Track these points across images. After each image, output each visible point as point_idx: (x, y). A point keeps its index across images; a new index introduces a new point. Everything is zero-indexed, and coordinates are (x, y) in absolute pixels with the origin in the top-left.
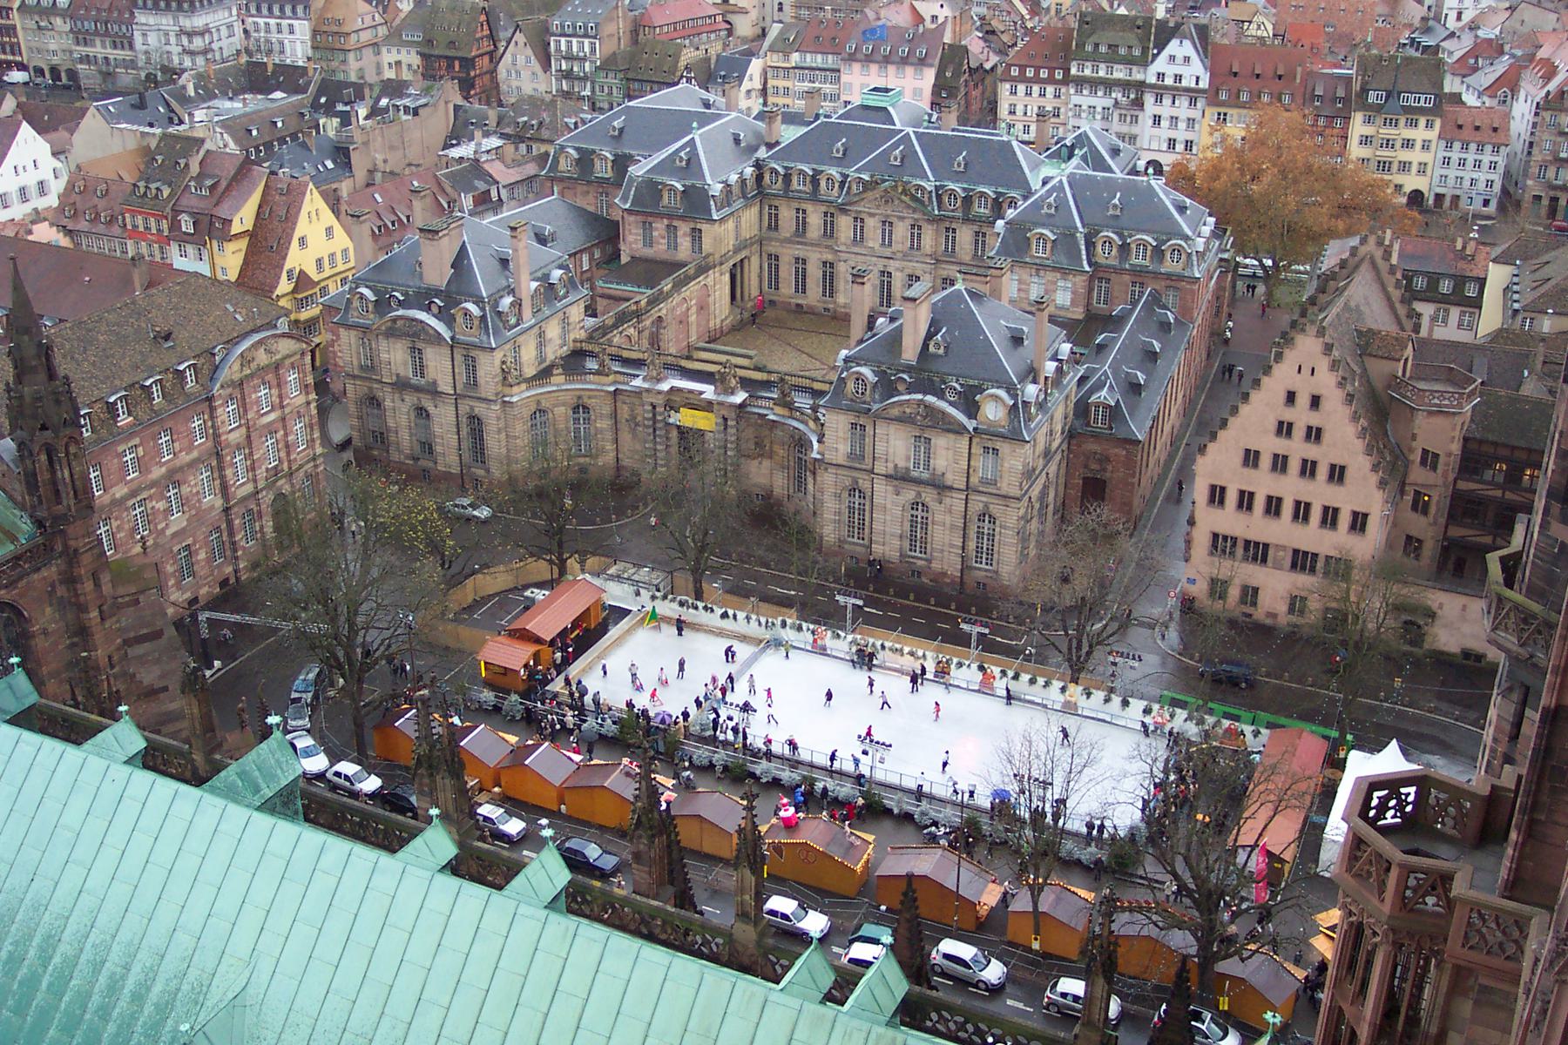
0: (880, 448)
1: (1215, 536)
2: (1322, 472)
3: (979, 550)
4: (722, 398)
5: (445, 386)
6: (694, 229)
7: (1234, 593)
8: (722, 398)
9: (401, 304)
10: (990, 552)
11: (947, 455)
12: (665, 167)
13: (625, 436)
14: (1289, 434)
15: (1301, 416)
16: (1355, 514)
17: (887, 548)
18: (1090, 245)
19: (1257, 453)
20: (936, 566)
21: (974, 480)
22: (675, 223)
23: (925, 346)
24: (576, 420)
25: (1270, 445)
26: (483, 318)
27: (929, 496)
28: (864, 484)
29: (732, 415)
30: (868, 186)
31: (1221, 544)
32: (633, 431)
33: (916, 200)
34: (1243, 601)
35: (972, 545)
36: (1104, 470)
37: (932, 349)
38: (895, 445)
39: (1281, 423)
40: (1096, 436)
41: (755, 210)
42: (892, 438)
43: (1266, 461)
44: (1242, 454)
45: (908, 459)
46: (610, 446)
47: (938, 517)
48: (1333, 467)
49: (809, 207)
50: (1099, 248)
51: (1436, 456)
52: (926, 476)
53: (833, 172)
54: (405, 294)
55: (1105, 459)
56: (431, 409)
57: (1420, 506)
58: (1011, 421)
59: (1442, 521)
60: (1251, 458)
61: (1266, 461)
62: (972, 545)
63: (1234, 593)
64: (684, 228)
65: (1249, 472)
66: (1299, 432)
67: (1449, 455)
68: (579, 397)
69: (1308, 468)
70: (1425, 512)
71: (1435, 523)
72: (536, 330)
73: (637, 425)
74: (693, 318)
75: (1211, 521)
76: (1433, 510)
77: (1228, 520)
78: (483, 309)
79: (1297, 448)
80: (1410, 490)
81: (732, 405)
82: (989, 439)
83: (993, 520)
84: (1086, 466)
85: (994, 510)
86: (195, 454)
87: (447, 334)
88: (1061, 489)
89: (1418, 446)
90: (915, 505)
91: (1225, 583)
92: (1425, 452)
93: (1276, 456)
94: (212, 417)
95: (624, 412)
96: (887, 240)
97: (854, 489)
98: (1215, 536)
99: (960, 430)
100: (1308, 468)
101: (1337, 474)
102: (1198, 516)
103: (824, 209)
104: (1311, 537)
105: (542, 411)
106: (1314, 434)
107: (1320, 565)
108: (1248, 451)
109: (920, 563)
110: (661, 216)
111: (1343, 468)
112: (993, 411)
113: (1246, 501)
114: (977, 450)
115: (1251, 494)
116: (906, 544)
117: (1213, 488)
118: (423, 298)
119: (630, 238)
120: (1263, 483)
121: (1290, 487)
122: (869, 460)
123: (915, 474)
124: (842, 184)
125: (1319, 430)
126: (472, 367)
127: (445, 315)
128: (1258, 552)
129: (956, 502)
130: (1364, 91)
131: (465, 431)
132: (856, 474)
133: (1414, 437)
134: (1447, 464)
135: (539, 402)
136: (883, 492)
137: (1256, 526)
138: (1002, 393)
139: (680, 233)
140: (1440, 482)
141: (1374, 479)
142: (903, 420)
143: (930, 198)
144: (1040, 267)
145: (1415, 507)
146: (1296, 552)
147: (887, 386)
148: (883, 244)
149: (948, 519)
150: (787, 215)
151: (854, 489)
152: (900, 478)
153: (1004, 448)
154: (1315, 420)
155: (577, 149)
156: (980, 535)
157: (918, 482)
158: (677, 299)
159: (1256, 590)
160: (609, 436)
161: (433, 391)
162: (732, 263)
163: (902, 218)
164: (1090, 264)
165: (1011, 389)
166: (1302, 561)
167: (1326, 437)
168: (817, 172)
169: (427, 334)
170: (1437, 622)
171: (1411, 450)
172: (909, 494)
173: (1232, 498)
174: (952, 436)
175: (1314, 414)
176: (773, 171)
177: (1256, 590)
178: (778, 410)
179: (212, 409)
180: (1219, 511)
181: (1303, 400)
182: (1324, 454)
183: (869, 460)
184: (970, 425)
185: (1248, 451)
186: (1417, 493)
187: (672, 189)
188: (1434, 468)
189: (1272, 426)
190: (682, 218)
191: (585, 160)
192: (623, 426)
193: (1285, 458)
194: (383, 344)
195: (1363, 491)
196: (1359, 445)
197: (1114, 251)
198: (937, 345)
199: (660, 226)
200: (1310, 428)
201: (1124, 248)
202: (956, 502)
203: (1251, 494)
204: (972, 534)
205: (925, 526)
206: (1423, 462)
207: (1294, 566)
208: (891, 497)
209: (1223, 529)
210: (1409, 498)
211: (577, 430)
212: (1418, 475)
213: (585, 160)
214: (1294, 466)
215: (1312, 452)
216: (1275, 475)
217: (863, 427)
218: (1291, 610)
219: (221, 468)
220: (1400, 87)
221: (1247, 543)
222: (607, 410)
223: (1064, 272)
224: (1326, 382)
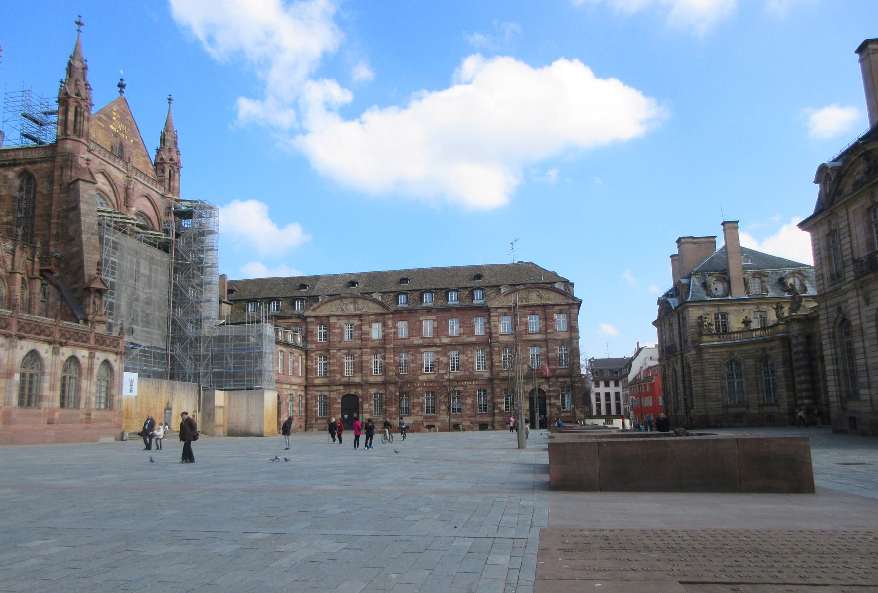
17: (873, 391)
42: (852, 225)
68: (764, 349)
86: (473, 339)
94: (489, 322)
105: (738, 364)
135: (731, 353)
179: (490, 317)
219: (491, 355)
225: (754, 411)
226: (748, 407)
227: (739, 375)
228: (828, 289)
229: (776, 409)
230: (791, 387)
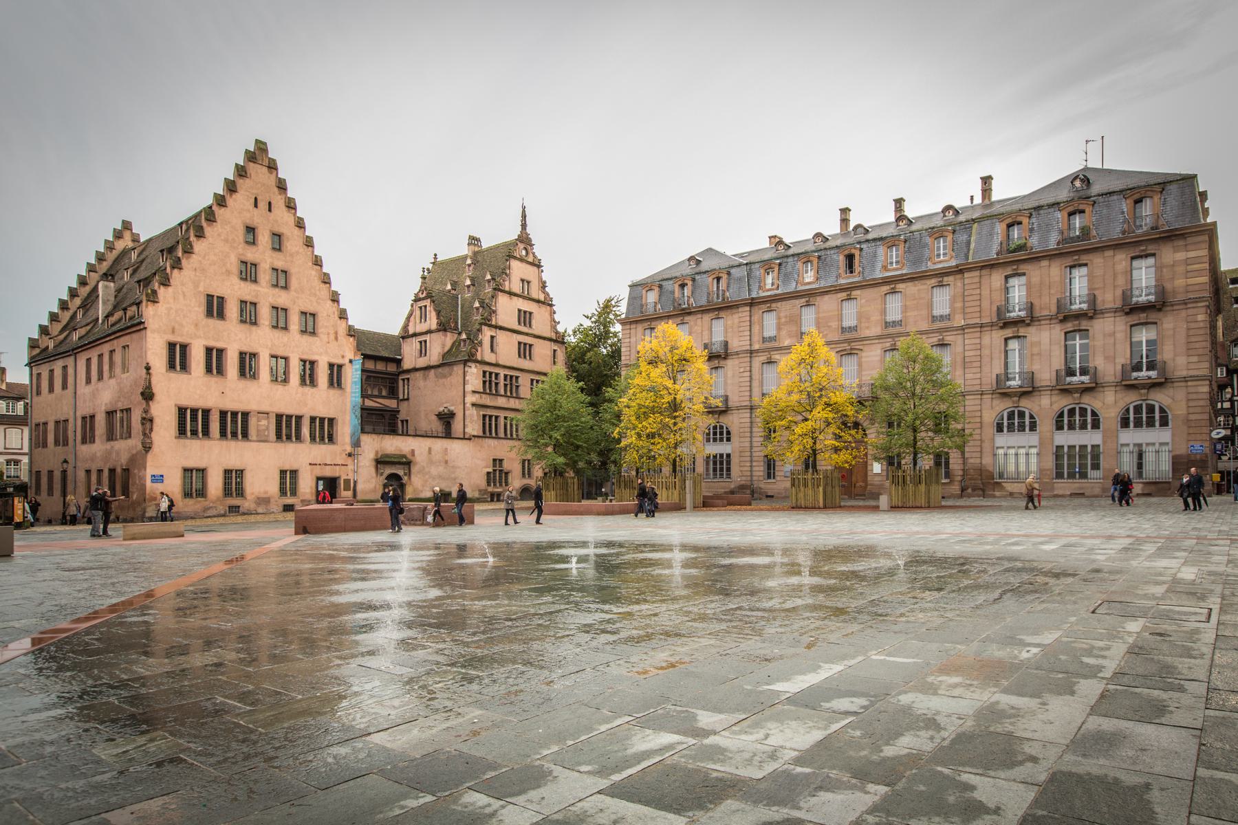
2: (295, 322)
7: (215, 484)
19: (221, 300)
25: (234, 290)
34: (227, 492)
44: (203, 300)
60: (215, 307)
61: (232, 310)
63: (215, 484)
66: (265, 276)
75: (176, 391)
77: (194, 387)
79: (265, 295)
98: (182, 411)
100: (280, 319)
102: (157, 388)
106: (282, 279)
107: (305, 431)
108: (210, 297)
113: (215, 360)
115: (221, 352)
120: (233, 337)
128: (235, 425)
137: (230, 393)
146: (279, 417)
159: (240, 473)
166: (287, 427)
170: (414, 469)
173: (197, 358)
177: (240, 473)
180: (183, 377)
181: (264, 238)
185: (210, 297)
203: (221, 352)
207: (279, 436)
209: (190, 401)
215: (282, 298)
218: (283, 492)
221: (223, 414)
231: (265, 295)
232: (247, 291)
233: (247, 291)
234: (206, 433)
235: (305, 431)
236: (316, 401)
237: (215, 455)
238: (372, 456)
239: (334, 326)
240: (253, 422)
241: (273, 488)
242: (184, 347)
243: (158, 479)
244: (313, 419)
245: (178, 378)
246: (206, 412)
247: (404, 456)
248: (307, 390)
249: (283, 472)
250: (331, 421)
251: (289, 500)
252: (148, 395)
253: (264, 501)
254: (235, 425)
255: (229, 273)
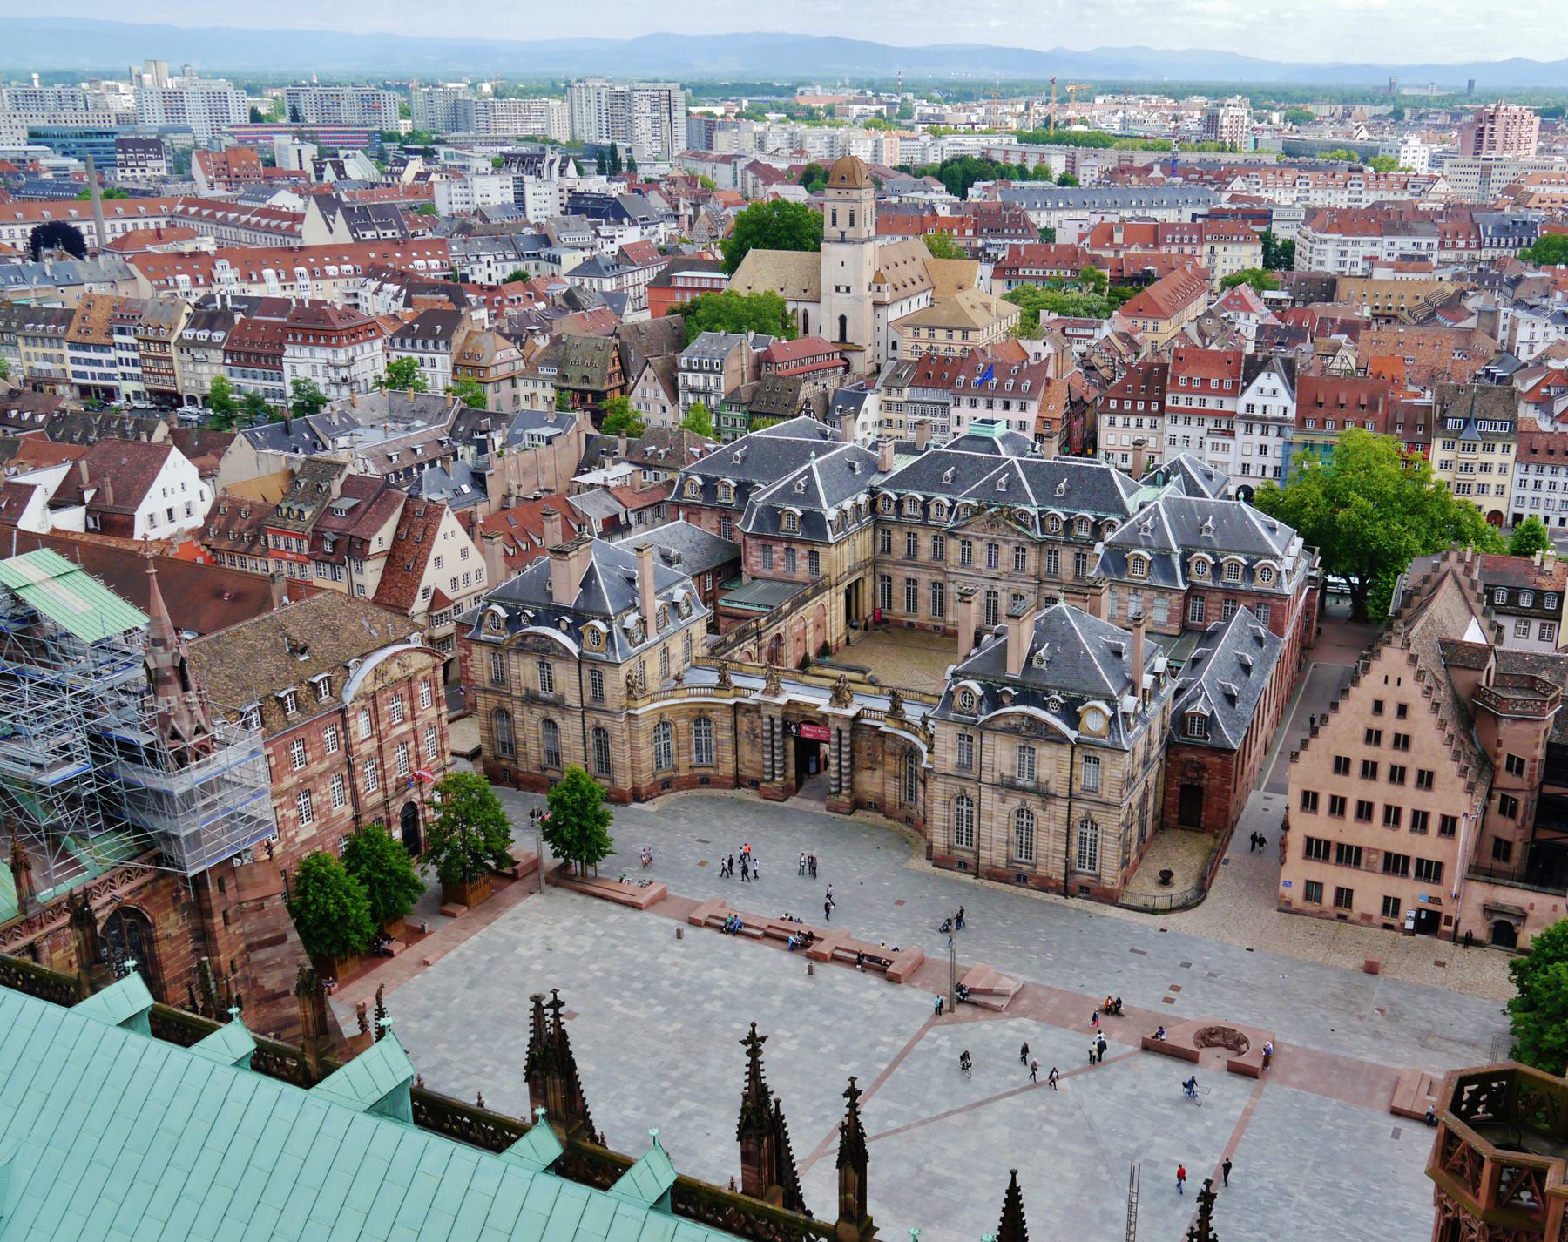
0: (987, 758)
1: (1309, 840)
2: (1411, 777)
3: (1082, 855)
4: (837, 711)
5: (572, 700)
6: (811, 553)
8: (837, 711)
9: (532, 621)
10: (1093, 857)
11: (1050, 764)
12: (787, 493)
13: (746, 751)
14: (1378, 741)
15: (1389, 724)
16: (1444, 818)
17: (994, 854)
18: (1185, 565)
19: (1347, 760)
20: (1041, 871)
21: (1076, 788)
22: (794, 546)
23: (1029, 661)
24: (698, 732)
25: (1359, 752)
26: (610, 635)
27: (1033, 803)
28: (972, 792)
29: (846, 727)
30: (977, 512)
31: (1316, 849)
32: (752, 743)
33: (1019, 519)
35: (1075, 850)
36: (1201, 778)
37: (1035, 664)
38: (1000, 755)
39: (1369, 732)
40: (1194, 747)
41: (869, 534)
42: (998, 747)
43: (1356, 768)
44: (1332, 760)
45: (1013, 768)
46: (729, 758)
47: (1043, 824)
48: (1421, 773)
49: (920, 532)
50: (1193, 568)
51: (1521, 761)
52: (1030, 784)
53: (944, 499)
54: (536, 612)
55: (1202, 767)
56: (559, 721)
57: (1508, 808)
58: (1111, 731)
59: (1530, 824)
60: (1342, 765)
61: (1356, 768)
62: (1075, 850)
63: (1329, 896)
64: (802, 551)
65: (1340, 779)
66: (1387, 740)
67: (1534, 760)
68: (701, 710)
69: (1397, 775)
70: (1513, 815)
71: (1523, 825)
72: (660, 647)
73: (756, 736)
74: (810, 636)
76: (1520, 813)
77: (1321, 825)
78: (610, 626)
79: (1386, 756)
80: (1498, 795)
81: (846, 718)
82: (1088, 751)
83: (1095, 826)
84: (1183, 774)
85: (1098, 815)
87: (574, 649)
88: (1160, 795)
89: (1504, 752)
90: (1020, 812)
91: (1320, 886)
92: (1510, 757)
93: (1366, 763)
95: (744, 722)
96: (993, 562)
97: (962, 798)
98: (1309, 840)
99: (1062, 740)
100: (1397, 775)
101: (1426, 780)
102: (1292, 823)
103: (934, 533)
104: (1402, 841)
106: (1402, 742)
107: (1412, 869)
108: (1338, 759)
109: (1025, 867)
110: (780, 540)
111: (1431, 774)
112: (1093, 723)
113: (1337, 806)
114: (1079, 759)
116: (1014, 851)
117: (1306, 794)
118: (551, 615)
119: (752, 560)
120: (1354, 789)
121: (1381, 792)
122: (976, 769)
123: (1020, 782)
124: (951, 510)
125: (1407, 738)
126: (598, 683)
127: (575, 633)
128: (1349, 856)
129: (1060, 809)
130: (1443, 419)
131: (591, 742)
132: (963, 783)
133: (1499, 743)
134: (1532, 769)
135: (662, 716)
136: (989, 800)
137: (1349, 831)
138: (1102, 705)
139: (798, 555)
140: (1526, 786)
141: (1462, 783)
142: (1011, 731)
143: (1034, 523)
144: (1137, 588)
145: (1502, 811)
146: (1388, 855)
147: (993, 699)
148: (989, 566)
149: (1052, 826)
150: (899, 538)
151: (962, 798)
152: (1008, 786)
153: (1105, 757)
154: (1402, 727)
155: (702, 477)
156: (1083, 840)
157: (1024, 790)
158: (795, 617)
159: (1350, 892)
160: (729, 746)
161: (559, 704)
162: (847, 583)
163: (1007, 542)
164: (1185, 582)
165: (1111, 702)
166: (1394, 864)
167: (1414, 744)
168: (927, 499)
169: (555, 648)
170: (1529, 922)
171: (1497, 756)
172: (1015, 802)
173: (1324, 803)
174: (1055, 746)
175: (1401, 722)
176: (886, 497)
177: (1350, 892)
178: (889, 722)
181: (1390, 709)
182: (1412, 761)
183: (976, 769)
184: (1073, 735)
185: (1338, 759)
186: (1503, 797)
187: (791, 514)
188: (1520, 772)
189: (1361, 734)
190: (800, 542)
191: (709, 487)
192: (743, 739)
193: (1375, 765)
194: (514, 659)
195: (1453, 795)
196: (1446, 752)
197: (1208, 571)
198: (1040, 660)
199: (779, 549)
200: (1397, 736)
201: (1217, 569)
202: (1060, 809)
204: (1075, 840)
205: (1030, 831)
206: (1509, 768)
208: (997, 805)
209: (1318, 833)
210: (1496, 802)
211: (698, 742)
212: (1506, 780)
213: (709, 487)
214: (1384, 771)
215: (1400, 758)
216: (1365, 782)
217: (970, 738)
218: (1385, 911)
220: (1476, 414)
221: (1340, 846)
222: (728, 722)
223: (1161, 591)
224: (1412, 692)
225: (684, 773)
226: (676, 769)
227: (666, 736)
228: (949, 771)
229: (712, 772)
230: (736, 752)
231: (1386, 756)
232: (1370, 753)
233: (1370, 753)
234: (1326, 857)
235: (1412, 869)
236: (1428, 846)
237: (1332, 876)
238: (1481, 900)
239: (1453, 783)
240: (1364, 855)
241: (1376, 909)
242: (1315, 795)
243: (1287, 884)
244: (1420, 861)
245: (1308, 818)
246: (1328, 843)
247: (1521, 909)
248: (1417, 836)
249: (1387, 899)
250: (1439, 865)
251: (1389, 920)
252: (1286, 826)
253: (1367, 917)
254: (1349, 856)
255: (1355, 739)
